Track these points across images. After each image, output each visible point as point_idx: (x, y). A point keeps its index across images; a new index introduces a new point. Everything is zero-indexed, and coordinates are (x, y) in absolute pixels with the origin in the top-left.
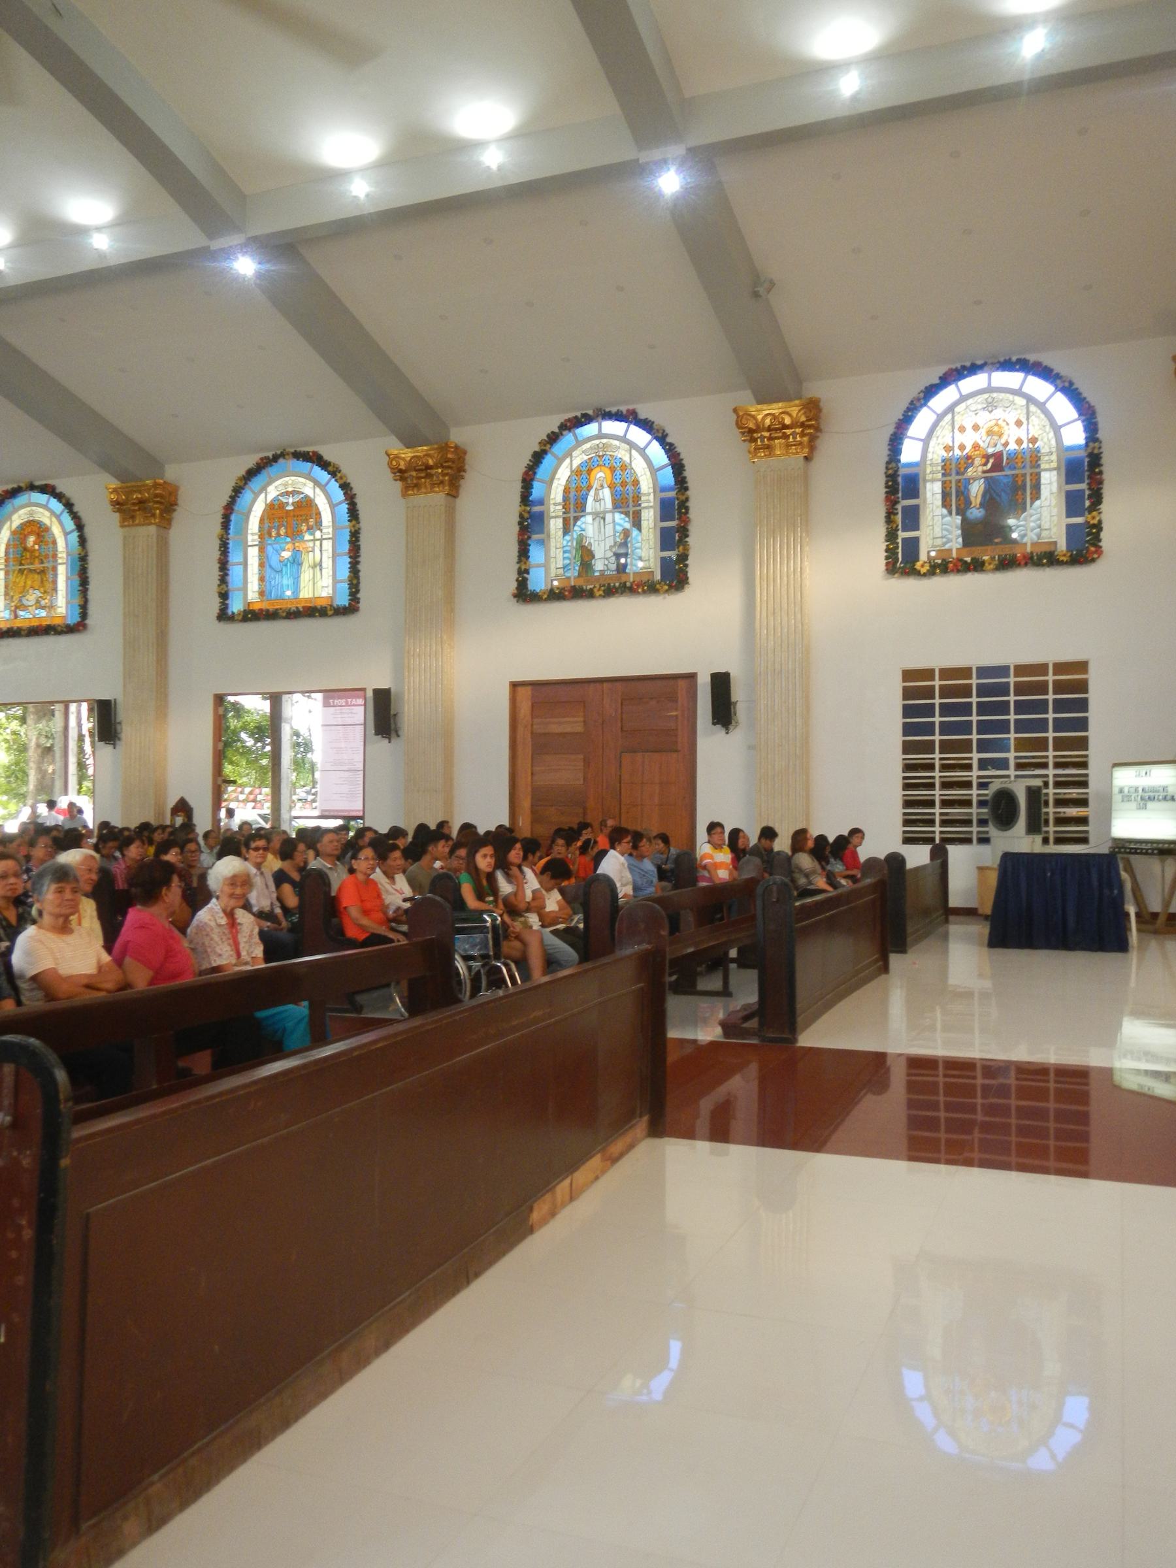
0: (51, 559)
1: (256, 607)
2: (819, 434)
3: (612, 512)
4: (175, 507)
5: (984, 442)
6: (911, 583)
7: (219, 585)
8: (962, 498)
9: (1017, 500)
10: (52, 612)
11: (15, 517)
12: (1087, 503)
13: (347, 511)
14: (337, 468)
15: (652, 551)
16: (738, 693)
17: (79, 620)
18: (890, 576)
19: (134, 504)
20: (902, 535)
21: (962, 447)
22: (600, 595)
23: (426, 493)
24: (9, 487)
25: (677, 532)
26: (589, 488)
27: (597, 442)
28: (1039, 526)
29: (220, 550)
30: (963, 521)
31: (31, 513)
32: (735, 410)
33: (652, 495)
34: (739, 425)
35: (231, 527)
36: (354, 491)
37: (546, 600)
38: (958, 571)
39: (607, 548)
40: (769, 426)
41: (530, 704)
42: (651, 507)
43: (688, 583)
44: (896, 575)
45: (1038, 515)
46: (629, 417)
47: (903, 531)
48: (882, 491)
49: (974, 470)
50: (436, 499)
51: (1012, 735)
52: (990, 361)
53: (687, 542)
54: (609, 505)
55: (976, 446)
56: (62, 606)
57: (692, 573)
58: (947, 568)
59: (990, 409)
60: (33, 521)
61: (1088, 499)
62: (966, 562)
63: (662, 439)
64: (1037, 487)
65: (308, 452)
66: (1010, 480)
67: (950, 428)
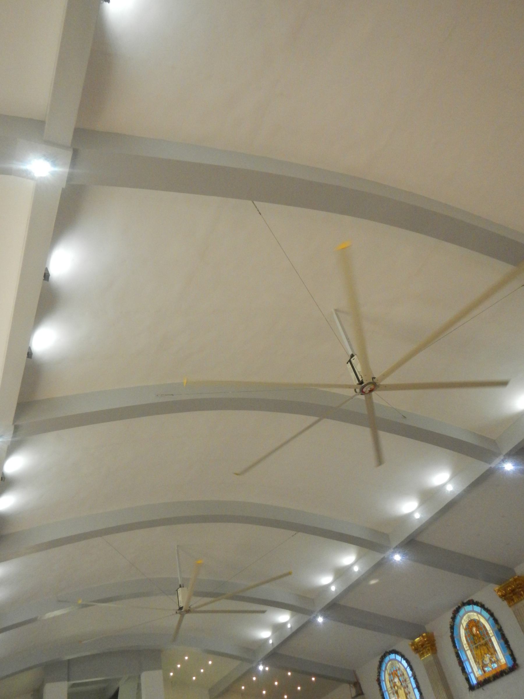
10: (499, 662)
11: (463, 621)
19: (510, 593)
24: (455, 608)
31: (469, 617)
56: (502, 658)
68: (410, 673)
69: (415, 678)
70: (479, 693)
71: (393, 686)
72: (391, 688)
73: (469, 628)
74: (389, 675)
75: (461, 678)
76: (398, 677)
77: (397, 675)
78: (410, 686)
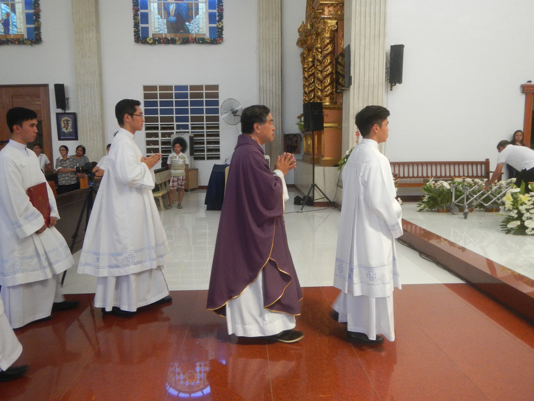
9: (189, 14)
12: (217, 18)
15: (22, 24)
18: (137, 43)
20: (141, 25)
25: (34, 15)
28: (199, 27)
30: (167, 21)
38: (165, 43)
42: (20, 2)
53: (39, 21)
57: (43, 36)
58: (161, 42)
61: (217, 17)
62: (168, 39)
64: (197, 9)
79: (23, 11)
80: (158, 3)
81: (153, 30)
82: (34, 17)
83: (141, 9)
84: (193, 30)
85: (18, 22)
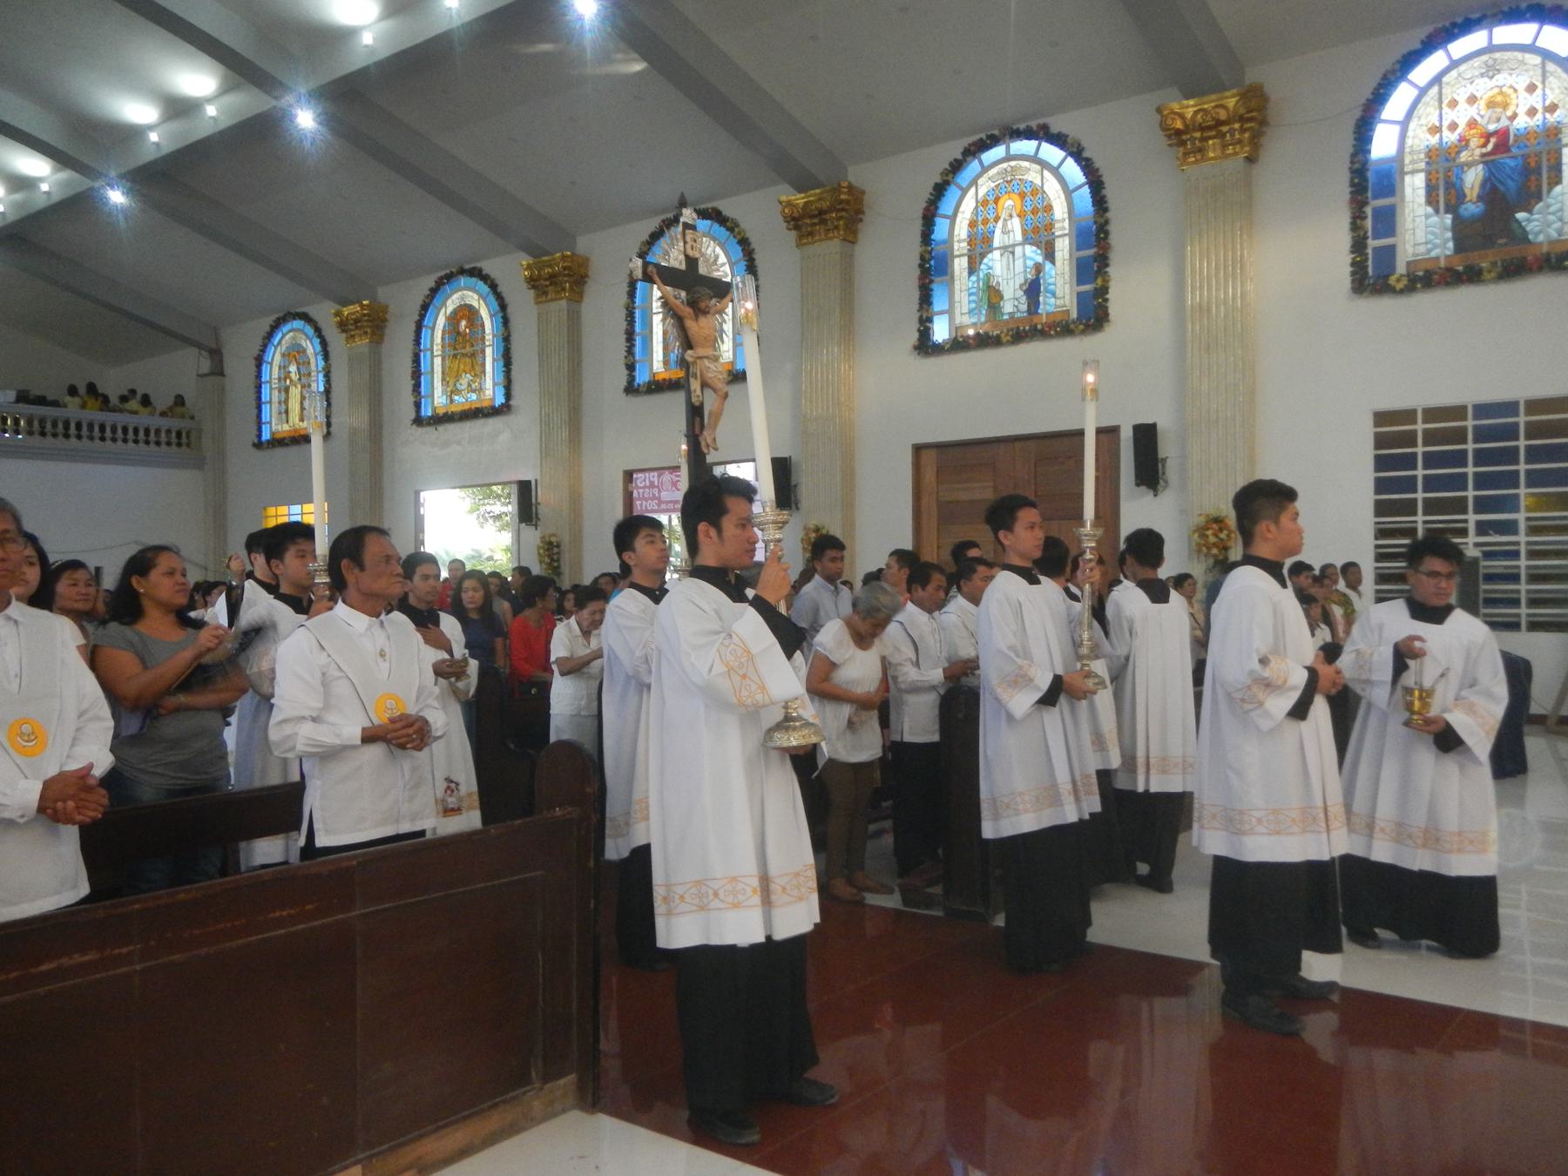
0: (480, 342)
1: (660, 377)
2: (1264, 129)
3: (1022, 244)
4: (586, 279)
5: (1482, 117)
6: (1385, 304)
7: (626, 357)
8: (1453, 191)
9: (1529, 187)
11: (449, 302)
13: (745, 268)
14: (735, 224)
15: (1067, 286)
16: (1167, 448)
17: (504, 401)
19: (546, 280)
20: (1372, 243)
21: (1453, 126)
22: (1008, 341)
23: (820, 240)
24: (442, 273)
26: (997, 219)
27: (1005, 165)
28: (1561, 220)
29: (626, 320)
30: (1454, 220)
31: (462, 299)
32: (1159, 110)
33: (1067, 221)
34: (1164, 127)
35: (637, 296)
36: (753, 246)
37: (948, 350)
39: (1017, 287)
40: (1200, 124)
41: (935, 469)
42: (1066, 235)
43: (1108, 321)
44: (1366, 294)
45: (1558, 205)
46: (1043, 133)
47: (1374, 239)
48: (1343, 190)
49: (1469, 154)
50: (829, 248)
51: (1523, 491)
52: (1489, 13)
53: (1106, 272)
54: (1019, 237)
55: (1472, 124)
56: (491, 390)
57: (1114, 308)
59: (1491, 74)
60: (466, 305)
62: (1458, 271)
63: (1077, 153)
65: (707, 209)
66: (1520, 161)
67: (1436, 104)
68: (321, 363)
69: (327, 376)
70: (429, 433)
71: (283, 376)
72: (279, 379)
73: (454, 319)
74: (283, 355)
75: (410, 399)
76: (298, 364)
77: (296, 360)
78: (314, 386)
79: (1071, 255)
80: (1426, 172)
81: (1410, 250)
82: (1096, 264)
83: (1375, 197)
84: (1537, 234)
85: (1060, 282)
